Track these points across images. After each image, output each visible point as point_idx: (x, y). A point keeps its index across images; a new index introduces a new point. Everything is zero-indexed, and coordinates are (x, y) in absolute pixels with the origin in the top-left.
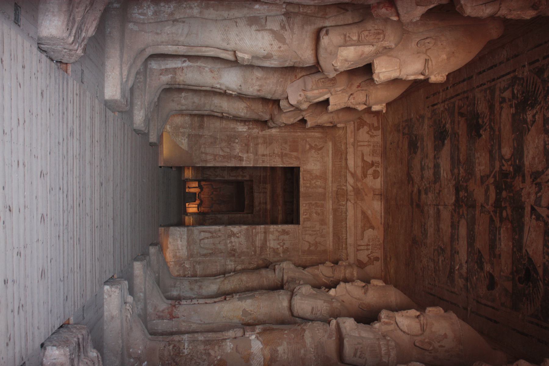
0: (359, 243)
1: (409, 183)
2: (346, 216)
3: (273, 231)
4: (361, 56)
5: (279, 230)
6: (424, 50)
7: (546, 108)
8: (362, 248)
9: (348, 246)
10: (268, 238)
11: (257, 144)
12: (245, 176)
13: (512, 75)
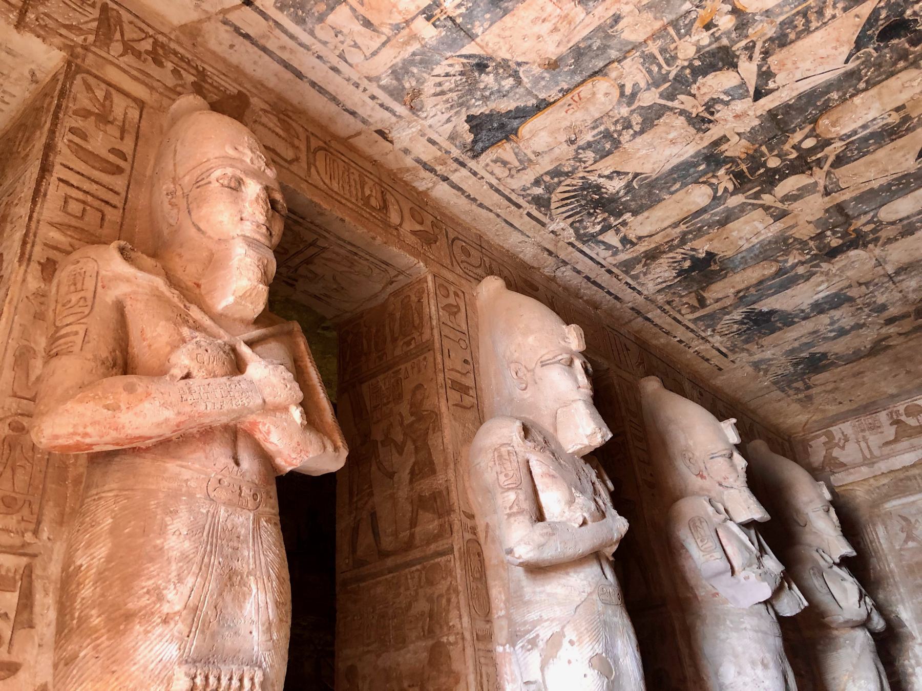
1: (888, 347)
4: (553, 476)
6: (529, 375)
7: (583, 165)
13: (579, 245)
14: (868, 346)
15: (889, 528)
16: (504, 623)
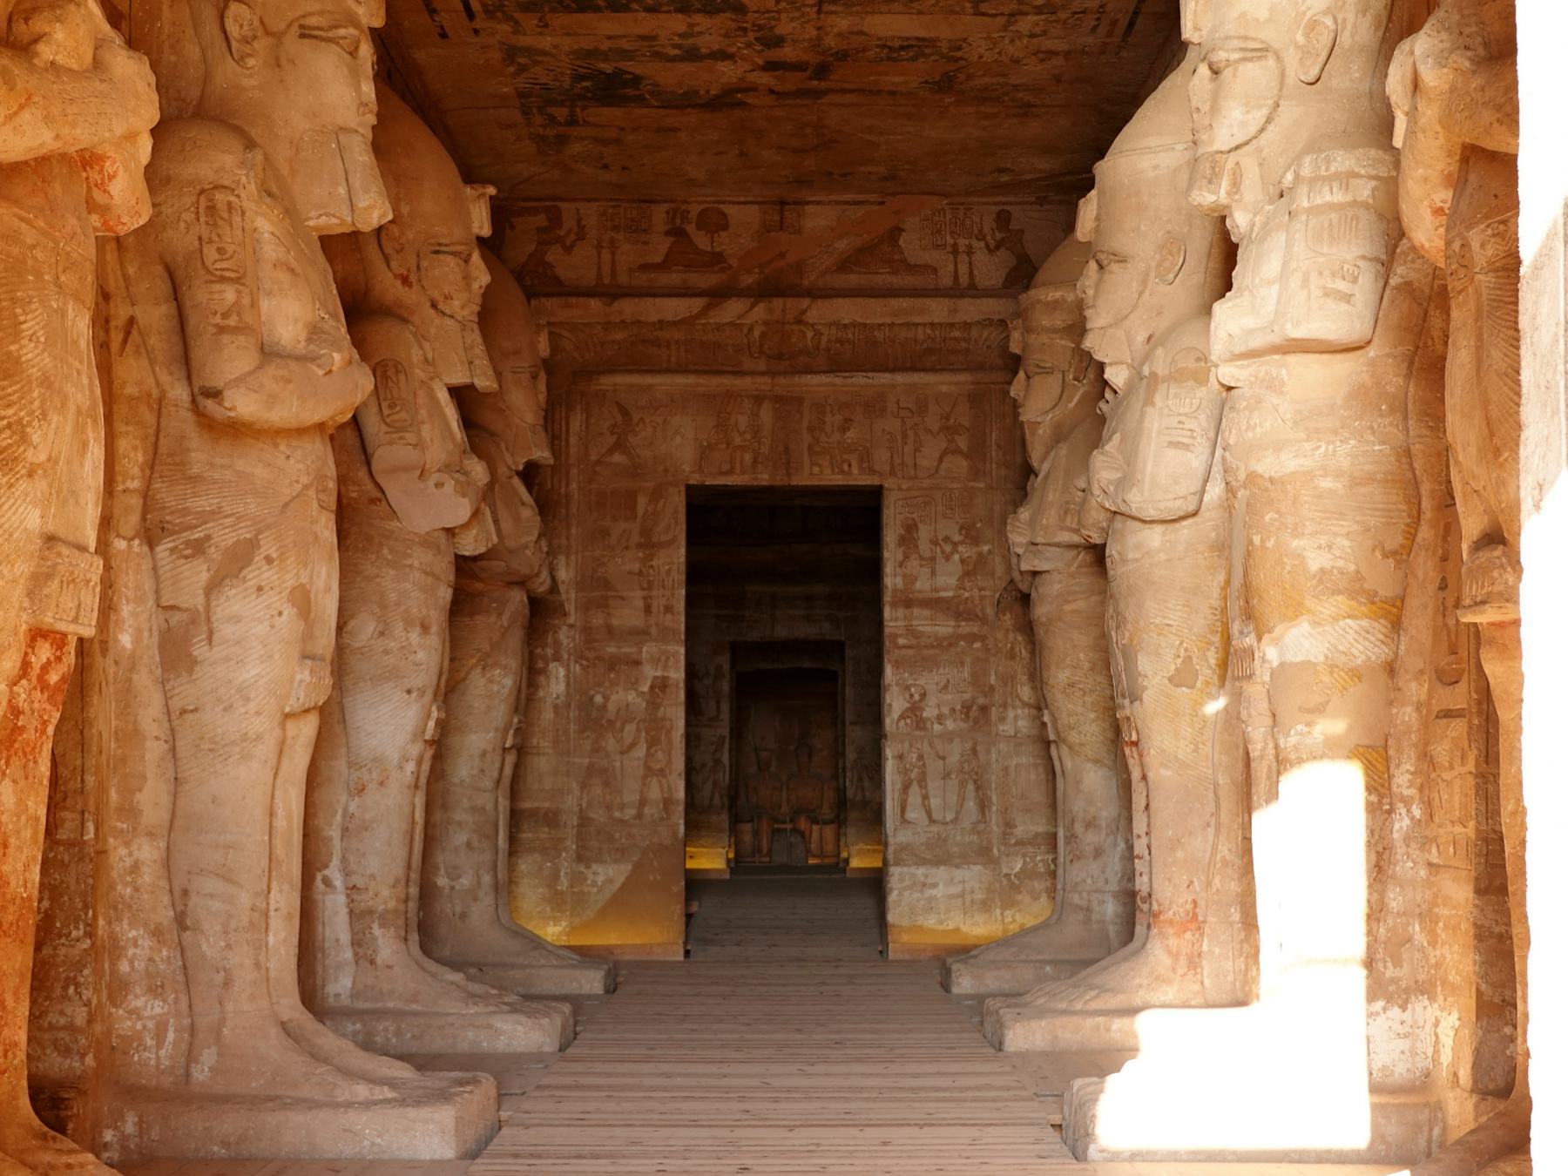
0: (946, 281)
1: (741, 104)
2: (854, 325)
3: (904, 576)
4: (292, 270)
5: (900, 556)
8: (963, 269)
9: (959, 318)
10: (927, 595)
11: (610, 631)
12: (719, 668)
14: (713, 92)
15: (593, 421)
16: (136, 501)
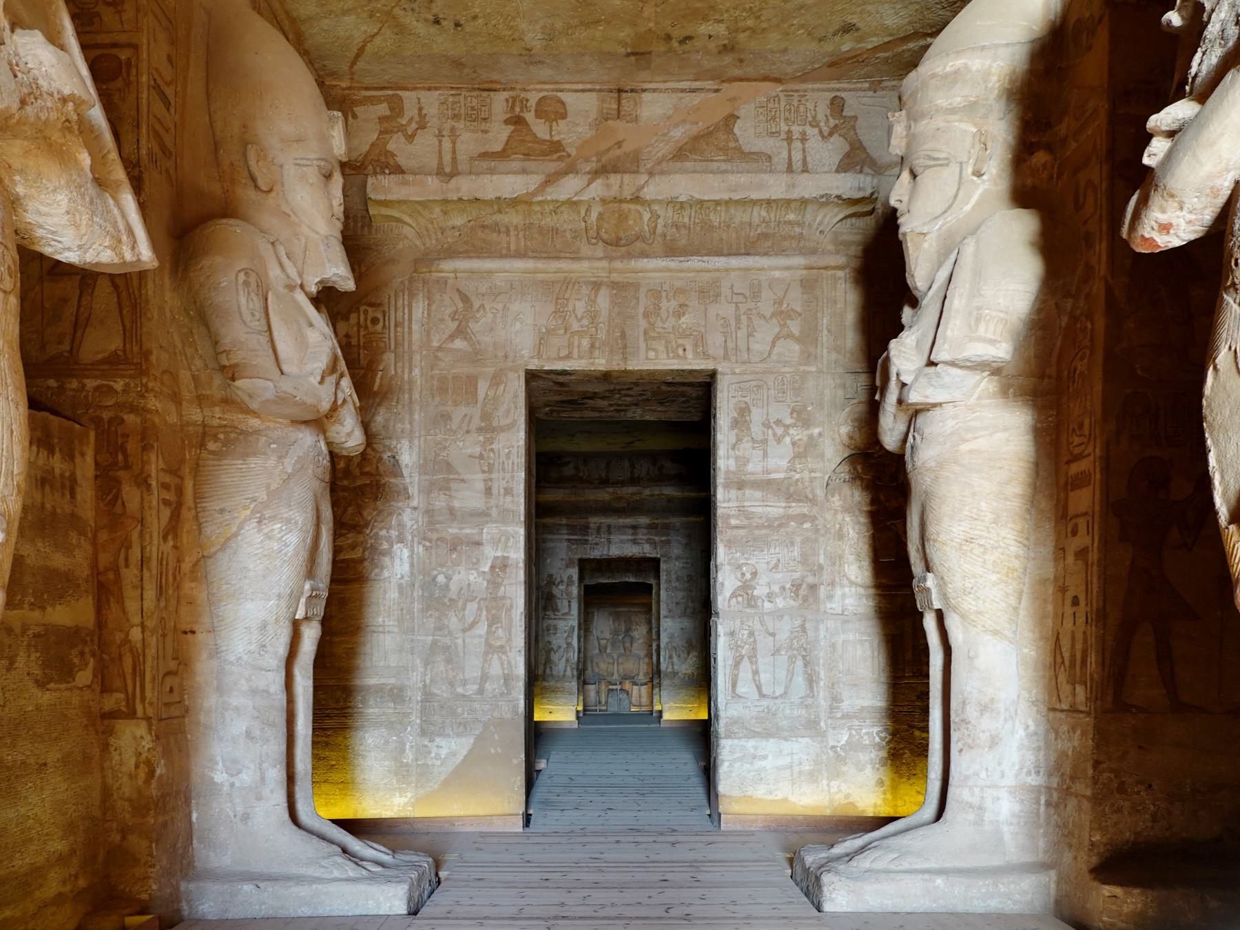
3: (737, 458)
10: (760, 477)
11: (451, 511)
12: (570, 577)
15: (434, 307)
